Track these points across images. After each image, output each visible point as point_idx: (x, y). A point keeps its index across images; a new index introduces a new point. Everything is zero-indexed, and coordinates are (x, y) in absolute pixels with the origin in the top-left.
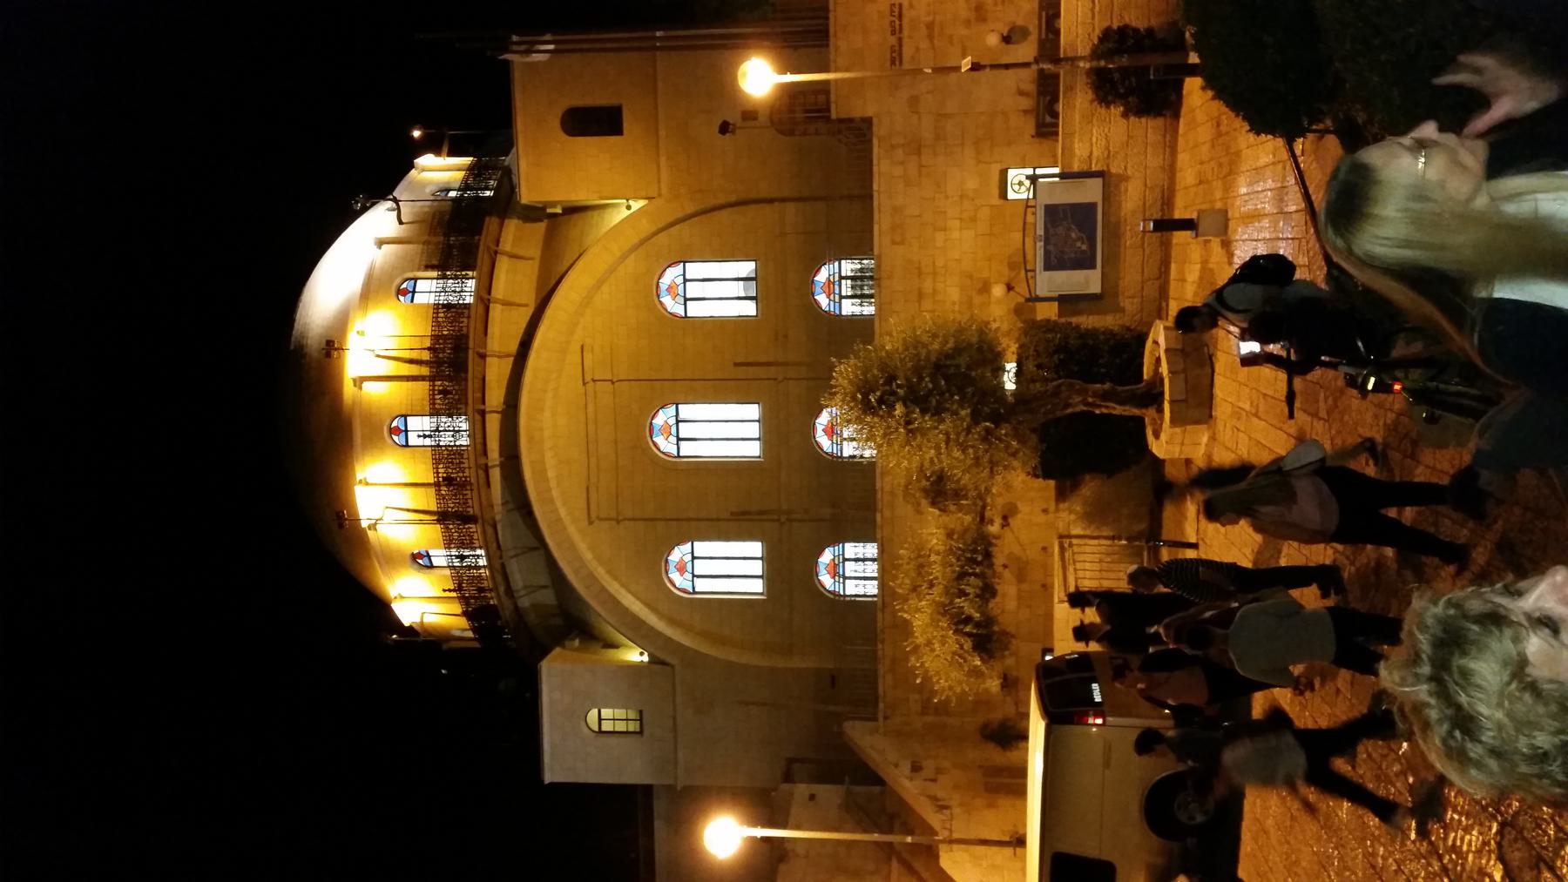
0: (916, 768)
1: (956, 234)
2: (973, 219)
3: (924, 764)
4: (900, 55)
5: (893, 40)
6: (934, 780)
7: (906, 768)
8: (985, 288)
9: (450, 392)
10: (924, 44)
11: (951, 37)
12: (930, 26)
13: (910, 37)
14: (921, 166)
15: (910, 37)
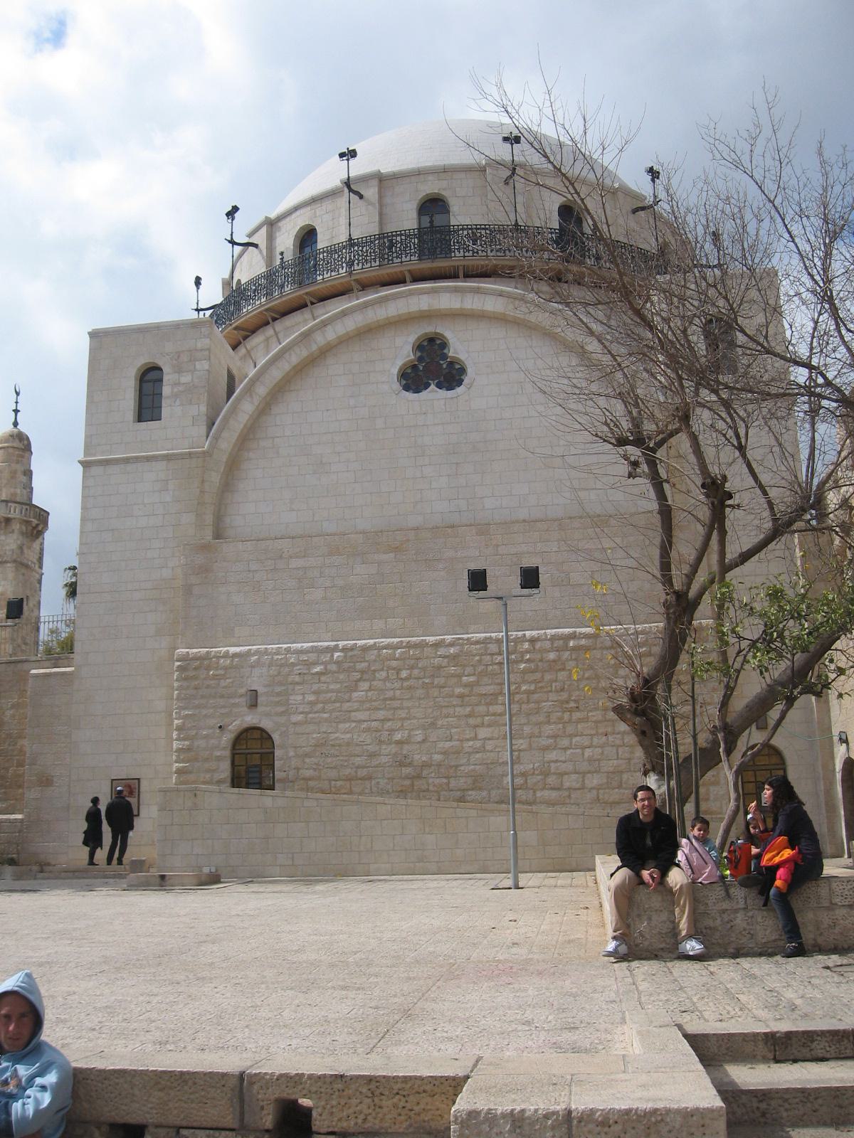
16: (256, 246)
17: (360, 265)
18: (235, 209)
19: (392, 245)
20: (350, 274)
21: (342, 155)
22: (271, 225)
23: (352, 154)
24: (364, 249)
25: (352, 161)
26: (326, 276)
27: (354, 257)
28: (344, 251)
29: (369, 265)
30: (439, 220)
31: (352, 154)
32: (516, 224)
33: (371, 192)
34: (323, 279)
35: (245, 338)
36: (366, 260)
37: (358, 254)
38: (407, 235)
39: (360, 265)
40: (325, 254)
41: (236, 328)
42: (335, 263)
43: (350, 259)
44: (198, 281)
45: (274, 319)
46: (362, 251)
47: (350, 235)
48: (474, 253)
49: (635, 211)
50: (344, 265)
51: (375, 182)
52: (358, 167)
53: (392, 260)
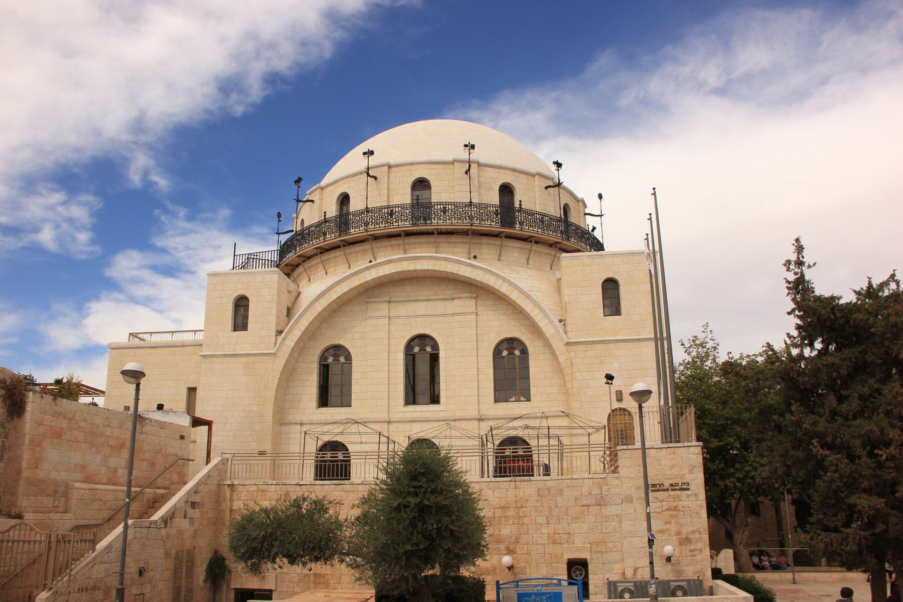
0: (194, 505)
1: (544, 531)
2: (554, 542)
3: (197, 511)
4: (658, 490)
5: (667, 484)
6: (185, 517)
7: (197, 498)
8: (510, 552)
9: (444, 213)
10: (665, 505)
11: (669, 522)
12: (676, 508)
13: (669, 496)
14: (589, 506)
15: (669, 496)
16: (313, 201)
18: (299, 180)
19: (391, 214)
20: (367, 231)
21: (364, 154)
22: (322, 189)
23: (371, 153)
30: (423, 194)
31: (371, 153)
32: (471, 202)
33: (381, 173)
35: (304, 261)
38: (403, 207)
41: (298, 256)
44: (279, 215)
45: (321, 253)
49: (547, 188)
51: (386, 168)
52: (373, 160)
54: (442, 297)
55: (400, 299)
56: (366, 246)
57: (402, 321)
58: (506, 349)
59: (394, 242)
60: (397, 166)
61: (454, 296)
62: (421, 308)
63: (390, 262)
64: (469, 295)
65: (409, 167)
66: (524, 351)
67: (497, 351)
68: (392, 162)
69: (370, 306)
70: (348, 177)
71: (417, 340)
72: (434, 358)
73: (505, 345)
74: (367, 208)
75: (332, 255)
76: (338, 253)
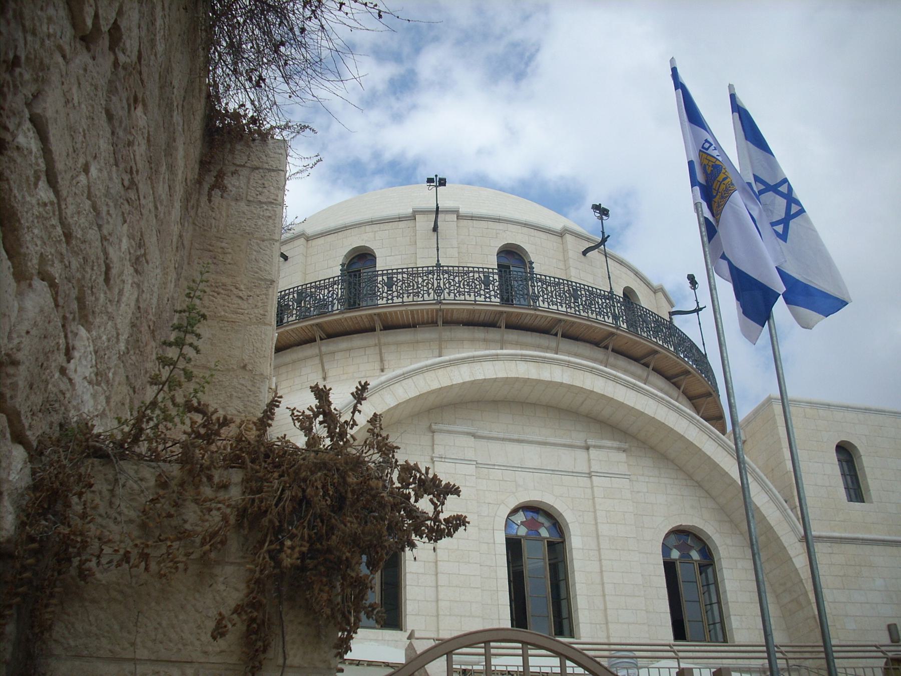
17: (452, 295)
21: (430, 181)
23: (442, 182)
24: (457, 279)
25: (440, 189)
26: (405, 299)
27: (444, 284)
28: (430, 276)
29: (462, 297)
31: (442, 182)
34: (403, 302)
36: (459, 292)
37: (450, 283)
39: (452, 295)
40: (405, 276)
42: (418, 287)
43: (439, 286)
45: (321, 339)
46: (453, 280)
47: (438, 261)
48: (575, 311)
50: (430, 291)
53: (490, 298)
54: (568, 441)
55: (494, 434)
56: (424, 334)
57: (497, 473)
58: (676, 547)
59: (479, 333)
60: (472, 218)
61: (591, 442)
62: (531, 455)
63: (496, 358)
64: (616, 444)
65: (491, 224)
66: (707, 554)
67: (666, 550)
68: (463, 210)
69: (438, 437)
70: (372, 222)
71: (521, 513)
72: (557, 550)
73: (673, 539)
74: (438, 265)
75: (343, 343)
76: (357, 341)
